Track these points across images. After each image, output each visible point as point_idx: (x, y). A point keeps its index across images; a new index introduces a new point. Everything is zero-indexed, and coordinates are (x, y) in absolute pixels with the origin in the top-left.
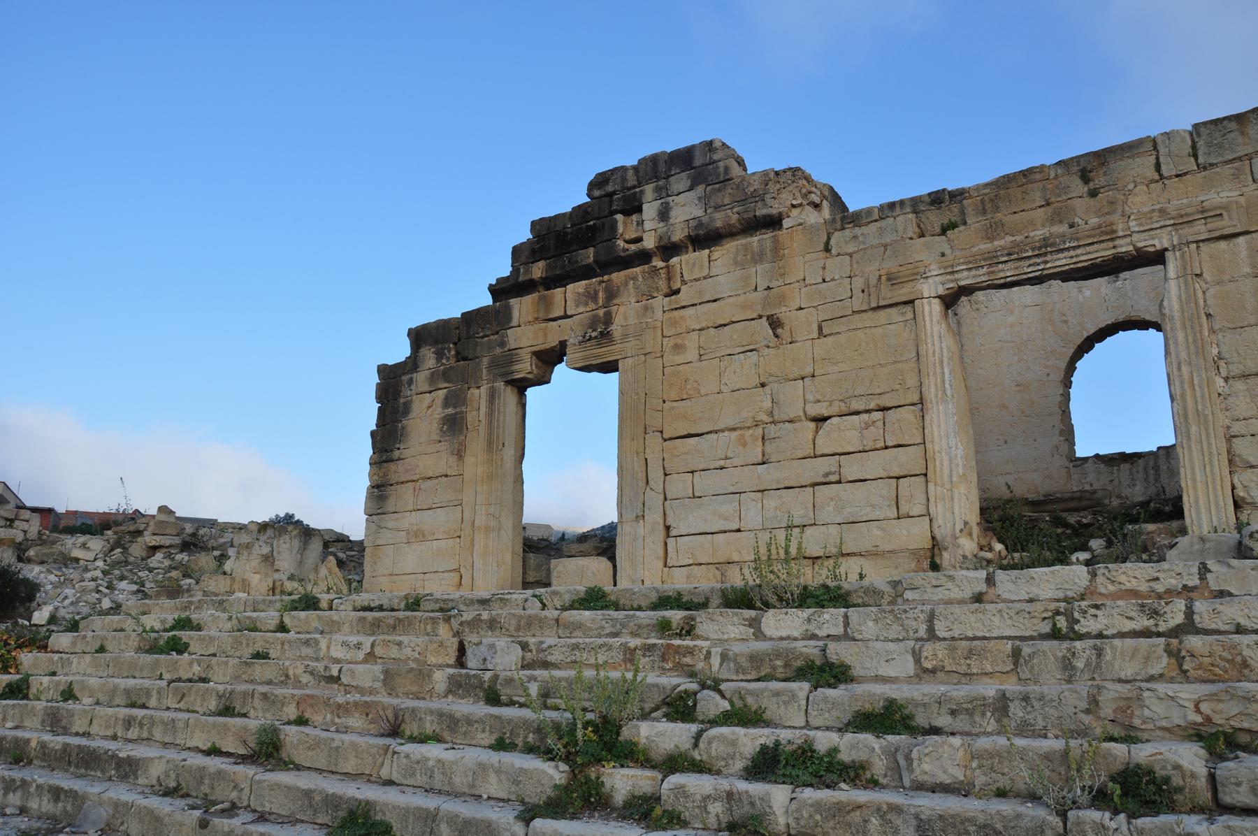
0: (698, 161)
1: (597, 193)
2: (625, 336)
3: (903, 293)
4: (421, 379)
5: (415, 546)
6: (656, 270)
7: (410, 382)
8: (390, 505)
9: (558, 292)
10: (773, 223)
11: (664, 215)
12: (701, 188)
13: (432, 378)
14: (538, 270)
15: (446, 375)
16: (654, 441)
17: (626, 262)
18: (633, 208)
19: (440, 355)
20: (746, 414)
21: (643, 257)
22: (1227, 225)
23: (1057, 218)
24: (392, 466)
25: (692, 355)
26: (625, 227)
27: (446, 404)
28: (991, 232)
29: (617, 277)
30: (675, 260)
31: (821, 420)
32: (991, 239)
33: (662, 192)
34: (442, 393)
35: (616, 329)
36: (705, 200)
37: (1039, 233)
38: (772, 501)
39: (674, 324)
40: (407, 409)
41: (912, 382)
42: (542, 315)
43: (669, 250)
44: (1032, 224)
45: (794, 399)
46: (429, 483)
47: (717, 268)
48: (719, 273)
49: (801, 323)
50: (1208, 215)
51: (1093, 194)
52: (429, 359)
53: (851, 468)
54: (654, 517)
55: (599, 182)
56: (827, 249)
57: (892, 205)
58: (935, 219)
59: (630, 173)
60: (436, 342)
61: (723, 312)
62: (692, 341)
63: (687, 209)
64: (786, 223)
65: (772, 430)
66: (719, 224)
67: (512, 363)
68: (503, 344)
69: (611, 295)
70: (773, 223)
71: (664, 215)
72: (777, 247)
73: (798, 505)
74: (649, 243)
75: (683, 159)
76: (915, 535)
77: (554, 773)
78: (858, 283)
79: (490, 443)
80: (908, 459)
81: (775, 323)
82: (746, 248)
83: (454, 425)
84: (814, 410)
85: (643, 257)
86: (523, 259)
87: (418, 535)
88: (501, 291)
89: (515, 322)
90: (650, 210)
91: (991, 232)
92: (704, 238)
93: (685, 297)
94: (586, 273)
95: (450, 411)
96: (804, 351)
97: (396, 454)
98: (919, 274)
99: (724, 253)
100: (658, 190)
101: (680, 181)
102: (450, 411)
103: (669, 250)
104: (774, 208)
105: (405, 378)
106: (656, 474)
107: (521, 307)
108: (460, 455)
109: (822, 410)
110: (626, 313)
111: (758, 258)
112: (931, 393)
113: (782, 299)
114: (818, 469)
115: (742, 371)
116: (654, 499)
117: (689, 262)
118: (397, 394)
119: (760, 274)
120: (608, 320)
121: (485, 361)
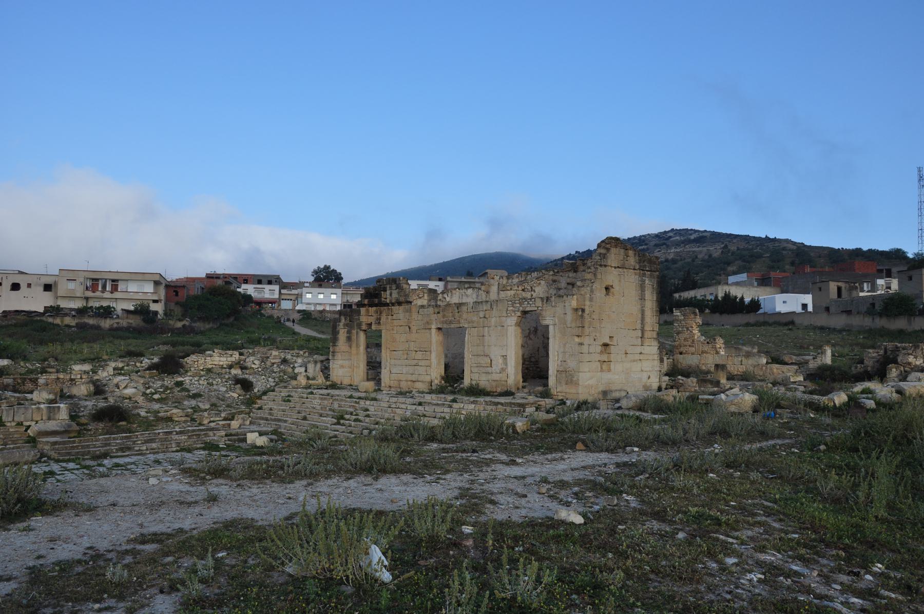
4: (341, 324)
11: (391, 295)
13: (344, 325)
22: (475, 325)
36: (398, 293)
43: (393, 304)
49: (414, 329)
50: (473, 322)
70: (411, 302)
71: (391, 295)
74: (388, 301)
76: (428, 379)
77: (335, 421)
80: (427, 363)
83: (349, 339)
85: (387, 305)
90: (388, 292)
91: (444, 316)
92: (399, 303)
93: (394, 317)
94: (376, 305)
98: (431, 324)
107: (363, 310)
108: (350, 347)
114: (414, 362)
116: (388, 364)
117: (395, 308)
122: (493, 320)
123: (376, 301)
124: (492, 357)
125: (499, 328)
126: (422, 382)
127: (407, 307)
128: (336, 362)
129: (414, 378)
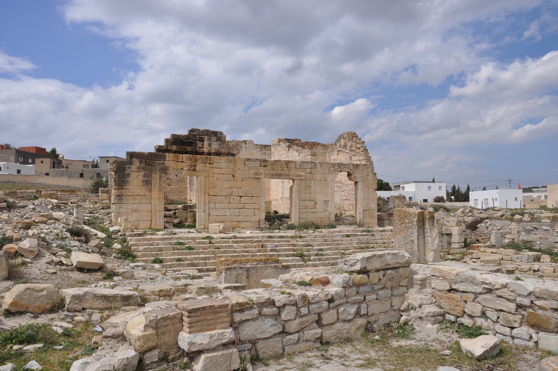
0: (218, 135)
2: (200, 171)
3: (258, 177)
4: (134, 168)
5: (135, 213)
6: (208, 158)
7: (129, 168)
8: (124, 201)
10: (233, 155)
11: (210, 145)
14: (174, 148)
15: (143, 168)
17: (197, 153)
18: (202, 140)
19: (141, 162)
21: (202, 153)
22: (303, 178)
23: (282, 170)
24: (124, 191)
25: (216, 179)
26: (199, 144)
27: (144, 176)
28: (273, 169)
29: (198, 156)
30: (212, 157)
31: (241, 197)
32: (272, 171)
33: (209, 140)
34: (142, 173)
35: (197, 168)
37: (280, 172)
38: (232, 211)
40: (129, 175)
42: (176, 160)
43: (209, 154)
44: (278, 170)
46: (137, 197)
47: (222, 161)
48: (222, 162)
50: (301, 176)
51: (287, 167)
52: (136, 162)
53: (247, 206)
54: (207, 211)
55: (192, 131)
56: (245, 164)
58: (263, 164)
60: (139, 158)
61: (223, 171)
62: (216, 176)
63: (215, 146)
64: (237, 156)
65: (232, 197)
66: (222, 152)
67: (167, 170)
68: (163, 164)
69: (196, 160)
70: (233, 155)
71: (210, 145)
72: (235, 161)
74: (205, 150)
75: (215, 133)
76: (257, 219)
79: (160, 189)
80: (257, 206)
81: (234, 176)
82: (228, 159)
83: (147, 182)
84: (240, 195)
85: (202, 153)
86: (169, 143)
87: (136, 211)
88: (159, 149)
89: (167, 159)
90: (206, 143)
92: (218, 154)
94: (187, 153)
95: (146, 179)
97: (125, 187)
98: (261, 174)
99: (223, 159)
100: (208, 138)
101: (214, 138)
102: (146, 179)
103: (209, 154)
104: (235, 152)
105: (127, 166)
107: (169, 156)
108: (150, 191)
110: (200, 166)
111: (231, 162)
114: (241, 205)
115: (226, 185)
117: (216, 158)
118: (124, 169)
119: (232, 166)
120: (195, 166)
121: (158, 168)
122: (318, 176)
123: (189, 149)
124: (318, 202)
125: (323, 181)
126: (250, 222)
127: (231, 158)
128: (124, 206)
129: (239, 219)
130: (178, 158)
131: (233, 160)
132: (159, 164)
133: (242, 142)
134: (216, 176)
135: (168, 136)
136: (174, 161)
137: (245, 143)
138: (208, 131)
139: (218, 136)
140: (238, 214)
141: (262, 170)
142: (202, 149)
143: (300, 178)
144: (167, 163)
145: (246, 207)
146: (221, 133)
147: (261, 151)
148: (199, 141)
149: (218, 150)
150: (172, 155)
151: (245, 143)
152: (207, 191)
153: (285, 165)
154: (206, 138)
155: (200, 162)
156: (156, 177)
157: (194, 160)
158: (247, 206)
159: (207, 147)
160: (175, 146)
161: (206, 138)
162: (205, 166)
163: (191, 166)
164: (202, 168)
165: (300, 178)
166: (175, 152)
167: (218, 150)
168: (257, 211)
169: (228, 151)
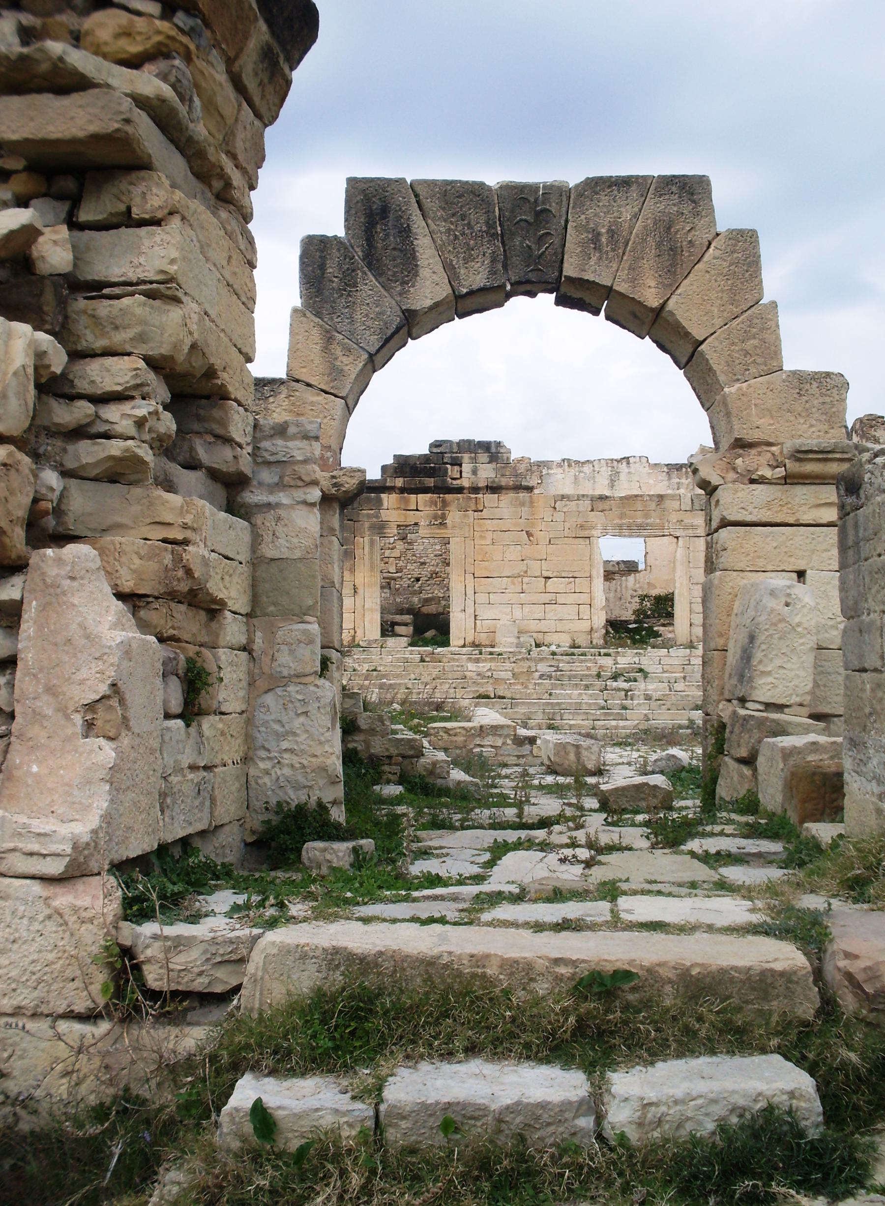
0: (493, 450)
1: (435, 450)
2: (454, 527)
3: (586, 533)
9: (413, 496)
11: (475, 472)
12: (493, 465)
14: (399, 482)
16: (470, 577)
18: (457, 463)
20: (516, 572)
21: (460, 490)
25: (489, 542)
26: (452, 471)
28: (622, 516)
29: (448, 497)
30: (480, 496)
32: (621, 518)
33: (474, 460)
37: (639, 521)
38: (527, 608)
39: (480, 526)
41: (587, 568)
42: (403, 507)
43: (475, 490)
45: (535, 568)
47: (502, 504)
48: (502, 506)
54: (470, 610)
57: (583, 496)
59: (455, 446)
61: (506, 525)
63: (487, 473)
64: (536, 491)
65: (525, 580)
66: (503, 484)
68: (377, 517)
69: (445, 504)
70: (530, 489)
71: (475, 472)
72: (532, 502)
73: (538, 612)
74: (465, 483)
75: (485, 446)
76: (585, 626)
78: (567, 525)
80: (584, 598)
81: (529, 534)
82: (517, 498)
84: (546, 574)
85: (460, 490)
89: (385, 505)
90: (467, 467)
91: (622, 516)
92: (494, 489)
94: (425, 490)
96: (542, 549)
98: (593, 528)
99: (507, 498)
100: (471, 458)
101: (483, 457)
103: (475, 490)
106: (470, 592)
109: (549, 574)
110: (453, 516)
111: (522, 504)
112: (594, 573)
113: (533, 525)
114: (547, 598)
115: (514, 553)
116: (470, 603)
117: (489, 499)
119: (525, 511)
120: (443, 517)
121: (367, 525)
123: (430, 482)
127: (523, 495)
130: (407, 502)
131: (528, 499)
132: (369, 516)
133: (618, 461)
134: (489, 535)
135: (390, 461)
136: (399, 508)
137: (628, 463)
138: (469, 442)
139: (491, 451)
140: (540, 615)
141: (597, 518)
142: (458, 482)
143: (690, 532)
144: (385, 515)
145: (559, 601)
146: (498, 444)
147: (669, 479)
148: (452, 465)
149: (494, 482)
150: (394, 497)
151: (628, 463)
152: (470, 569)
153: (653, 505)
154: (466, 457)
155: (453, 507)
156: (363, 542)
157: (439, 505)
158: (561, 599)
159: (469, 475)
160: (401, 479)
161: (466, 457)
162: (465, 516)
163: (435, 517)
164: (457, 520)
165: (690, 532)
166: (402, 490)
167: (494, 482)
168: (585, 609)
169: (513, 480)
